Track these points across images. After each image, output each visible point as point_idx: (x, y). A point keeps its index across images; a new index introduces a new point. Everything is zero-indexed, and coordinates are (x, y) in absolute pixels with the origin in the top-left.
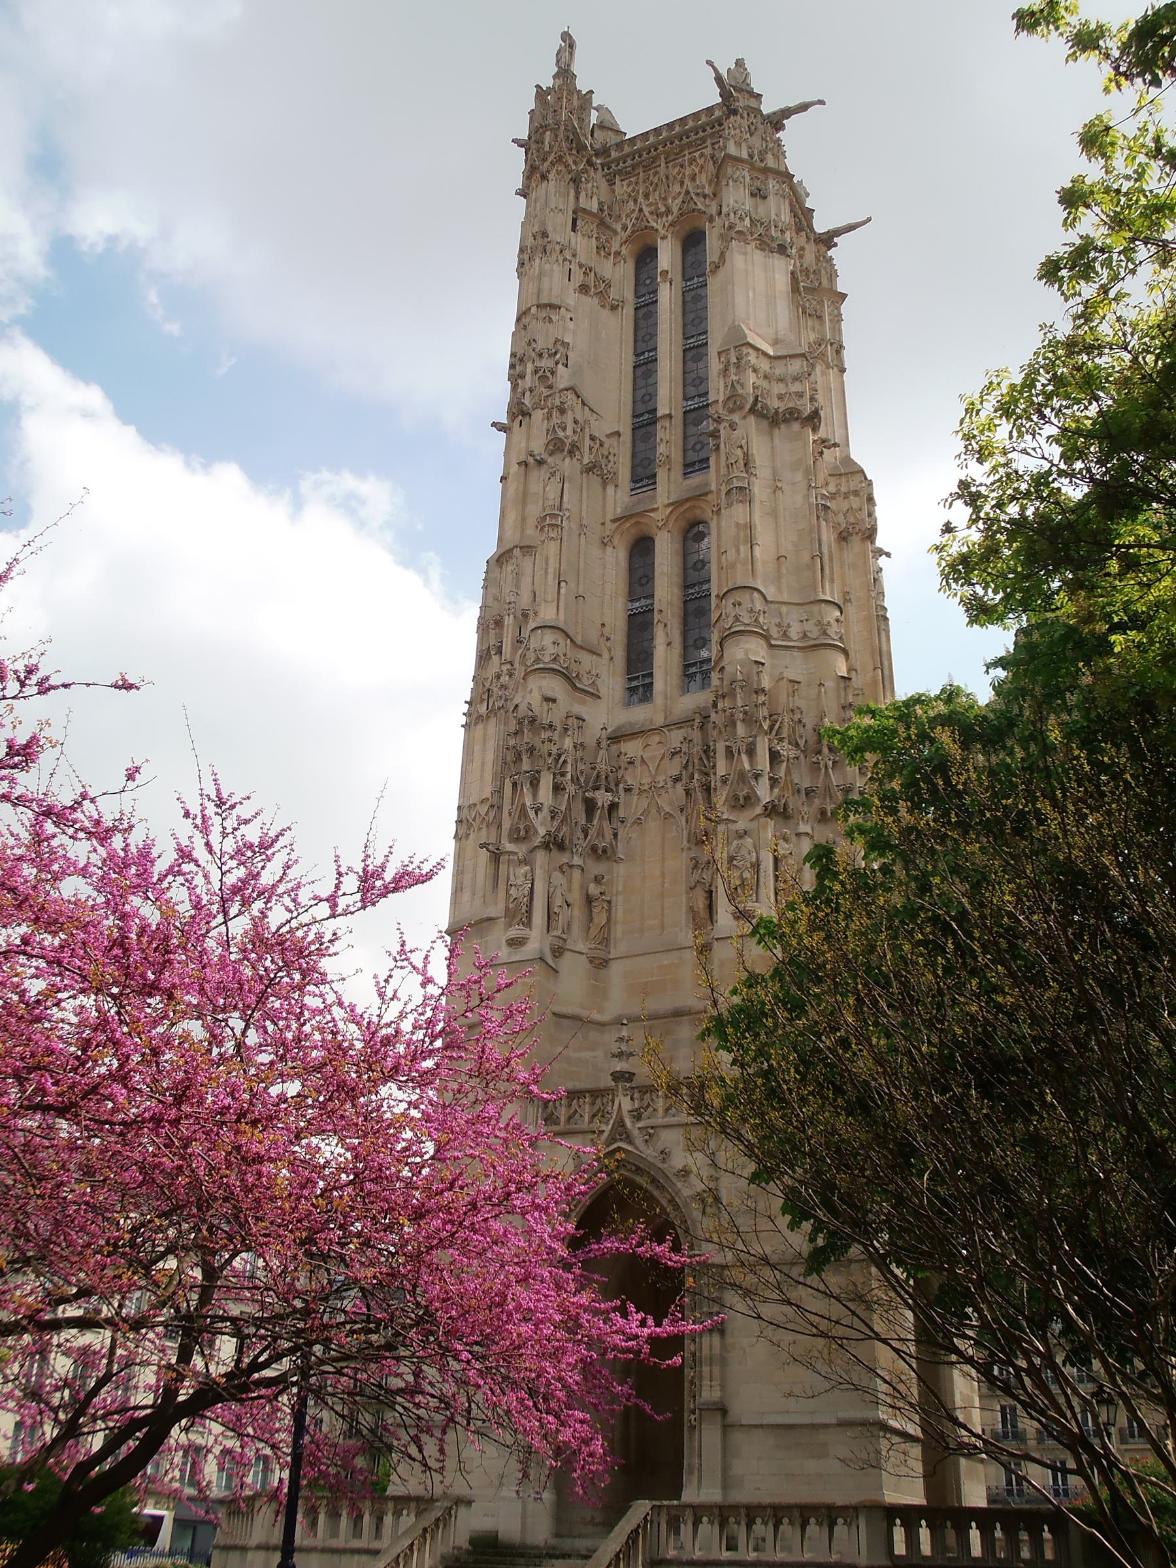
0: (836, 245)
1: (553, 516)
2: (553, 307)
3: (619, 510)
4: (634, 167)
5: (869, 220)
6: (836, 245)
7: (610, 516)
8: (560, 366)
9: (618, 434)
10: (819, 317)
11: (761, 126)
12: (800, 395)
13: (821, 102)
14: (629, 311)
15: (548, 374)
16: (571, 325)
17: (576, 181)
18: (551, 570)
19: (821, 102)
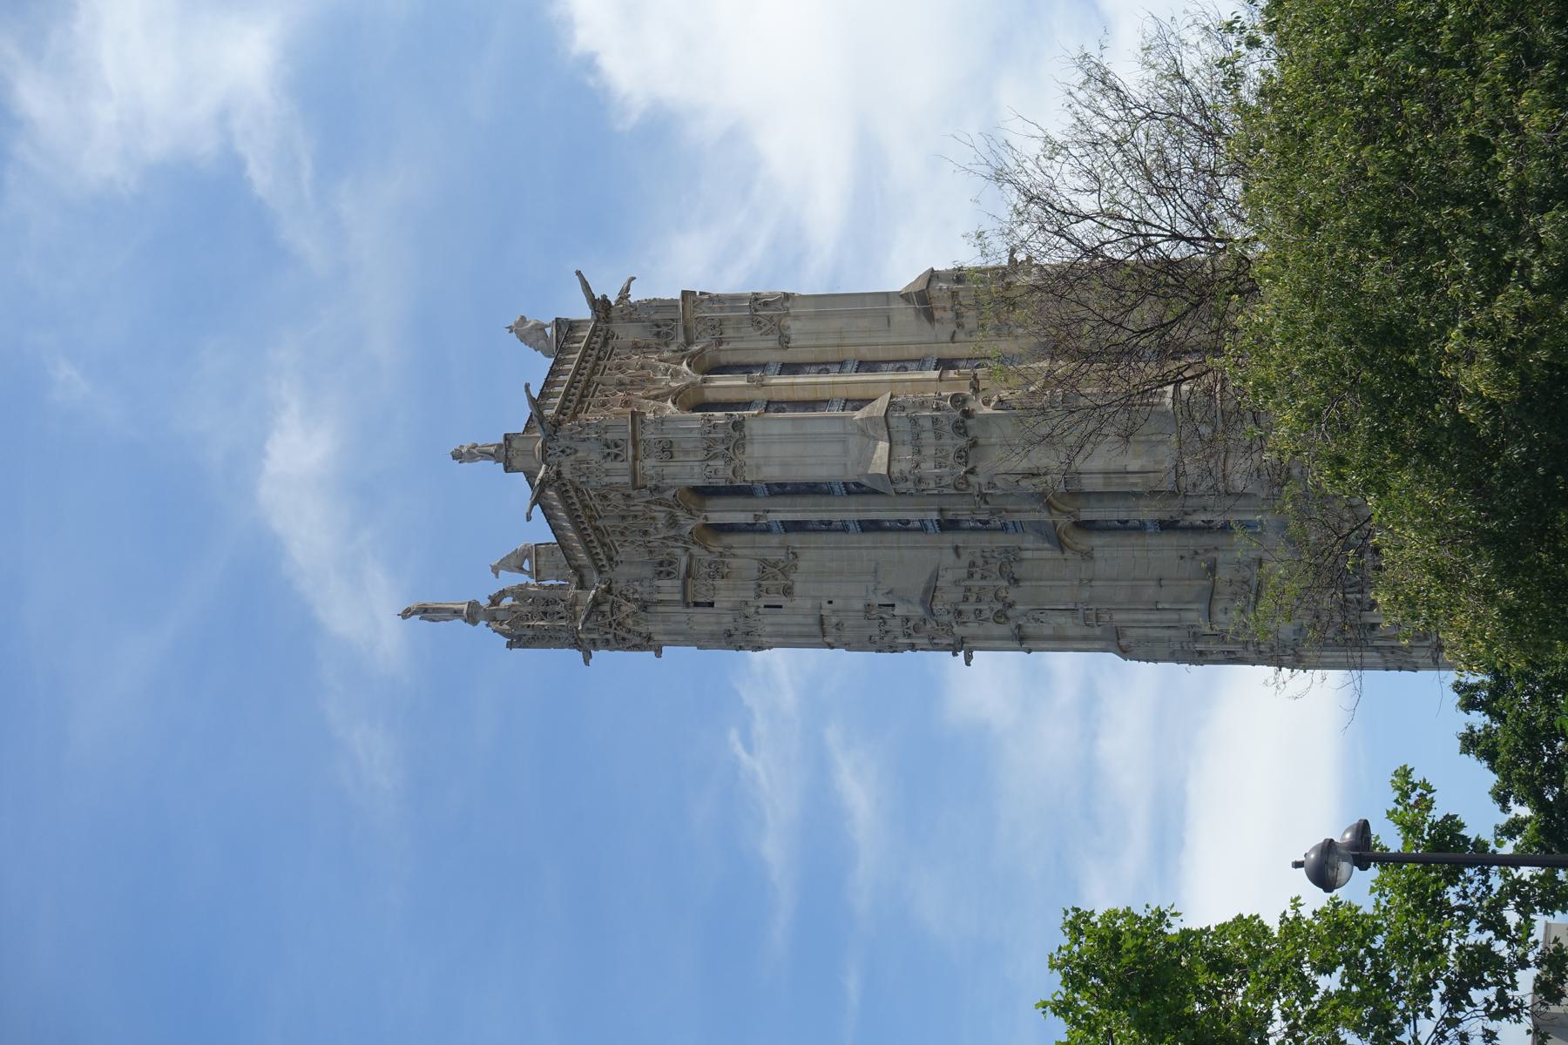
0: (604, 297)
1: (1086, 618)
2: (822, 623)
3: (1047, 545)
4: (603, 545)
5: (579, 273)
6: (604, 297)
7: (1058, 554)
8: (896, 612)
9: (956, 549)
10: (721, 321)
11: (562, 442)
12: (935, 420)
13: (527, 386)
14: (794, 539)
15: (911, 624)
16: (838, 603)
17: (645, 607)
18: (1145, 617)
19: (527, 386)
